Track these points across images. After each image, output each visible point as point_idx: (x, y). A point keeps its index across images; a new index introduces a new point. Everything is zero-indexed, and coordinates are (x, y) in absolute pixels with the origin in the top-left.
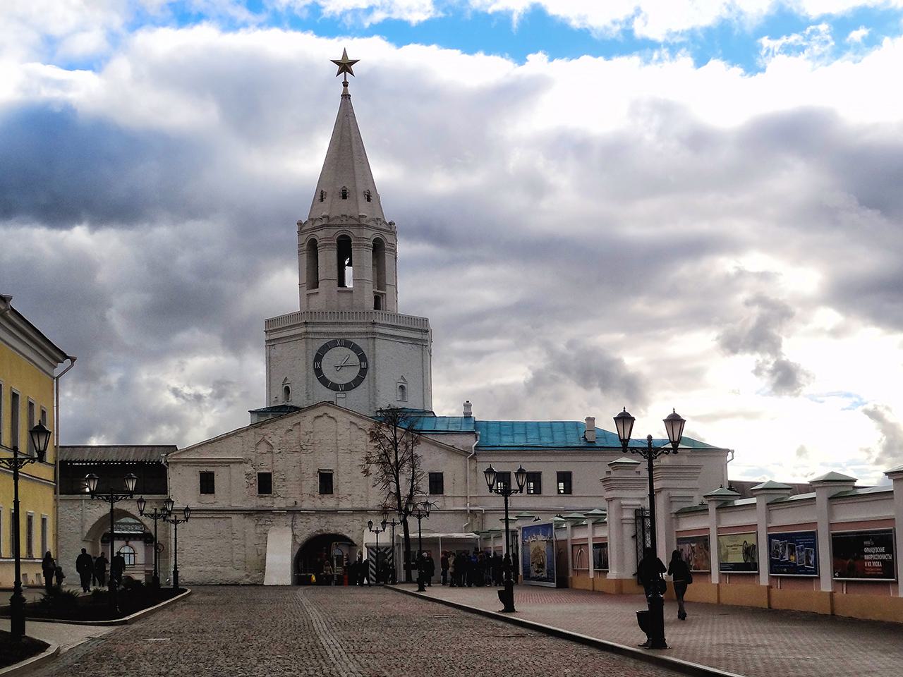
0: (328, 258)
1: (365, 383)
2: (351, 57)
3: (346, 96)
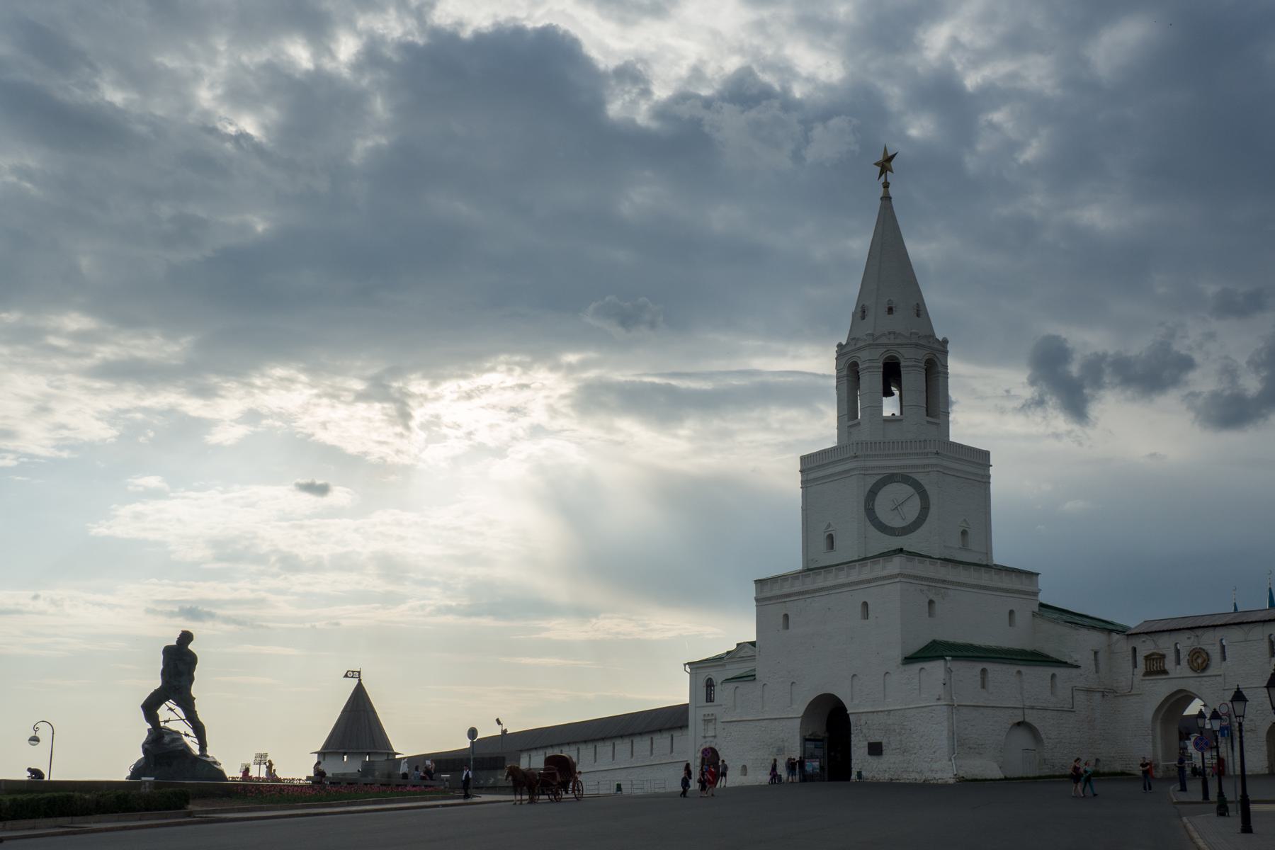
0: (872, 379)
2: (890, 154)
3: (886, 198)
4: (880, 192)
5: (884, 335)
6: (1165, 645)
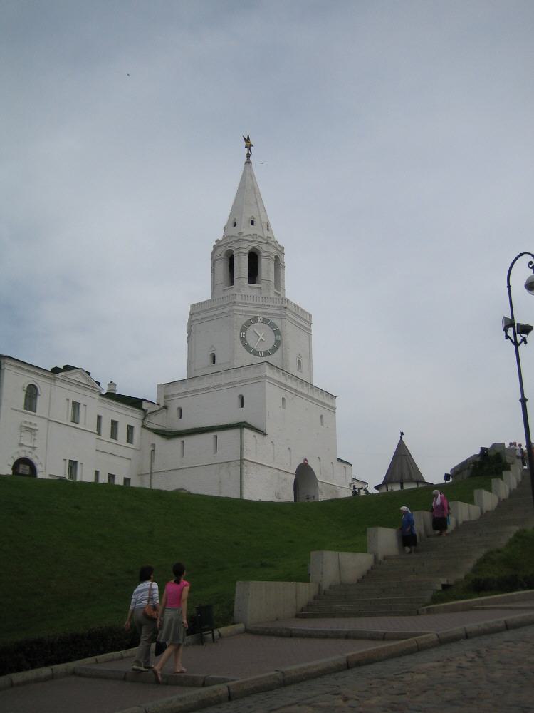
1: (279, 351)
3: (248, 162)
5: (250, 235)
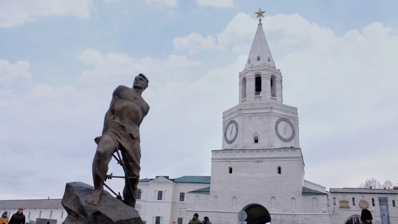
2: (262, 11)
4: (258, 22)
6: (349, 198)
